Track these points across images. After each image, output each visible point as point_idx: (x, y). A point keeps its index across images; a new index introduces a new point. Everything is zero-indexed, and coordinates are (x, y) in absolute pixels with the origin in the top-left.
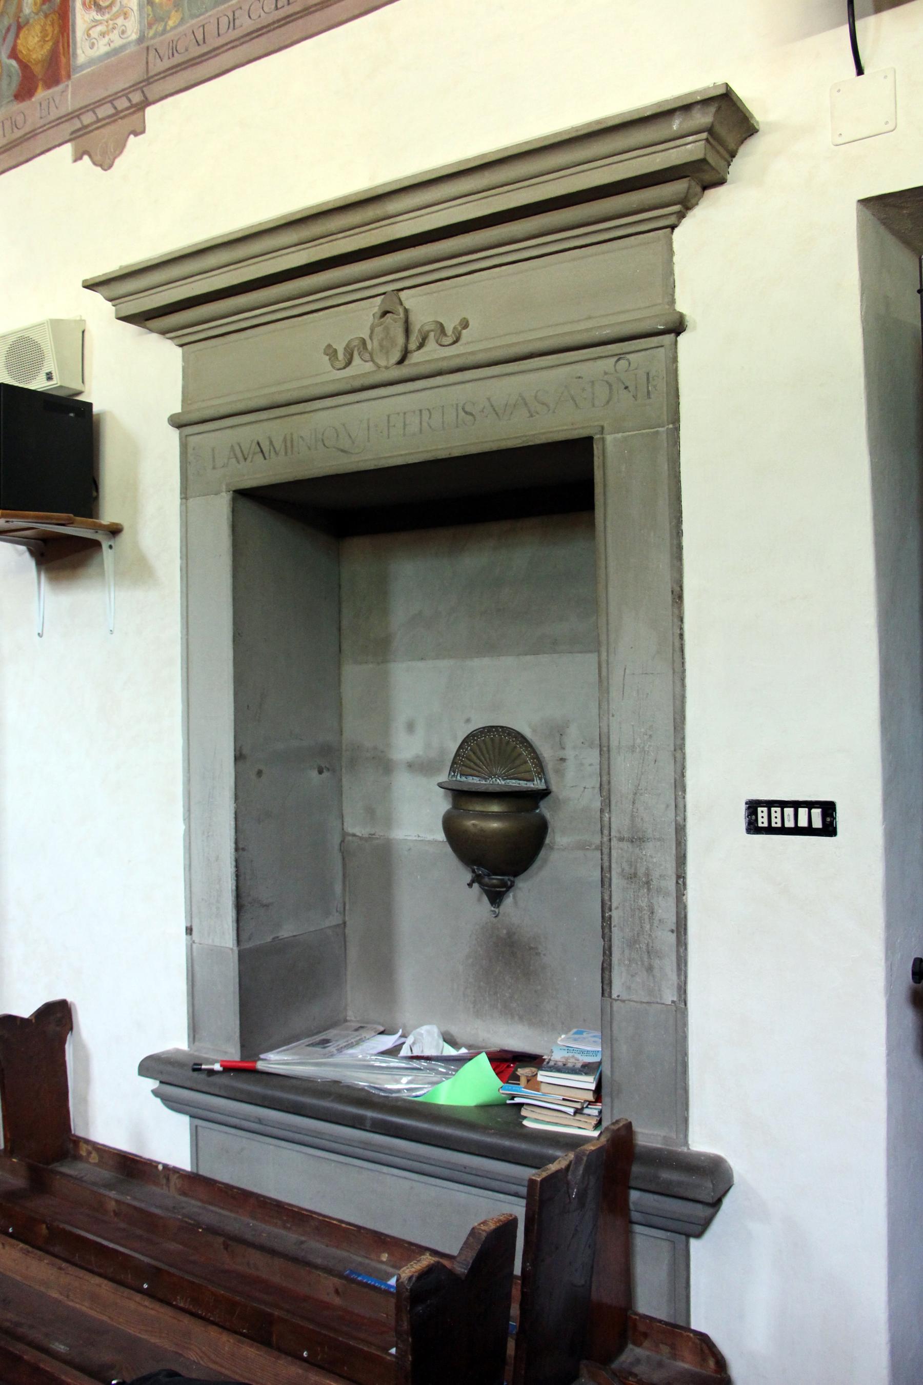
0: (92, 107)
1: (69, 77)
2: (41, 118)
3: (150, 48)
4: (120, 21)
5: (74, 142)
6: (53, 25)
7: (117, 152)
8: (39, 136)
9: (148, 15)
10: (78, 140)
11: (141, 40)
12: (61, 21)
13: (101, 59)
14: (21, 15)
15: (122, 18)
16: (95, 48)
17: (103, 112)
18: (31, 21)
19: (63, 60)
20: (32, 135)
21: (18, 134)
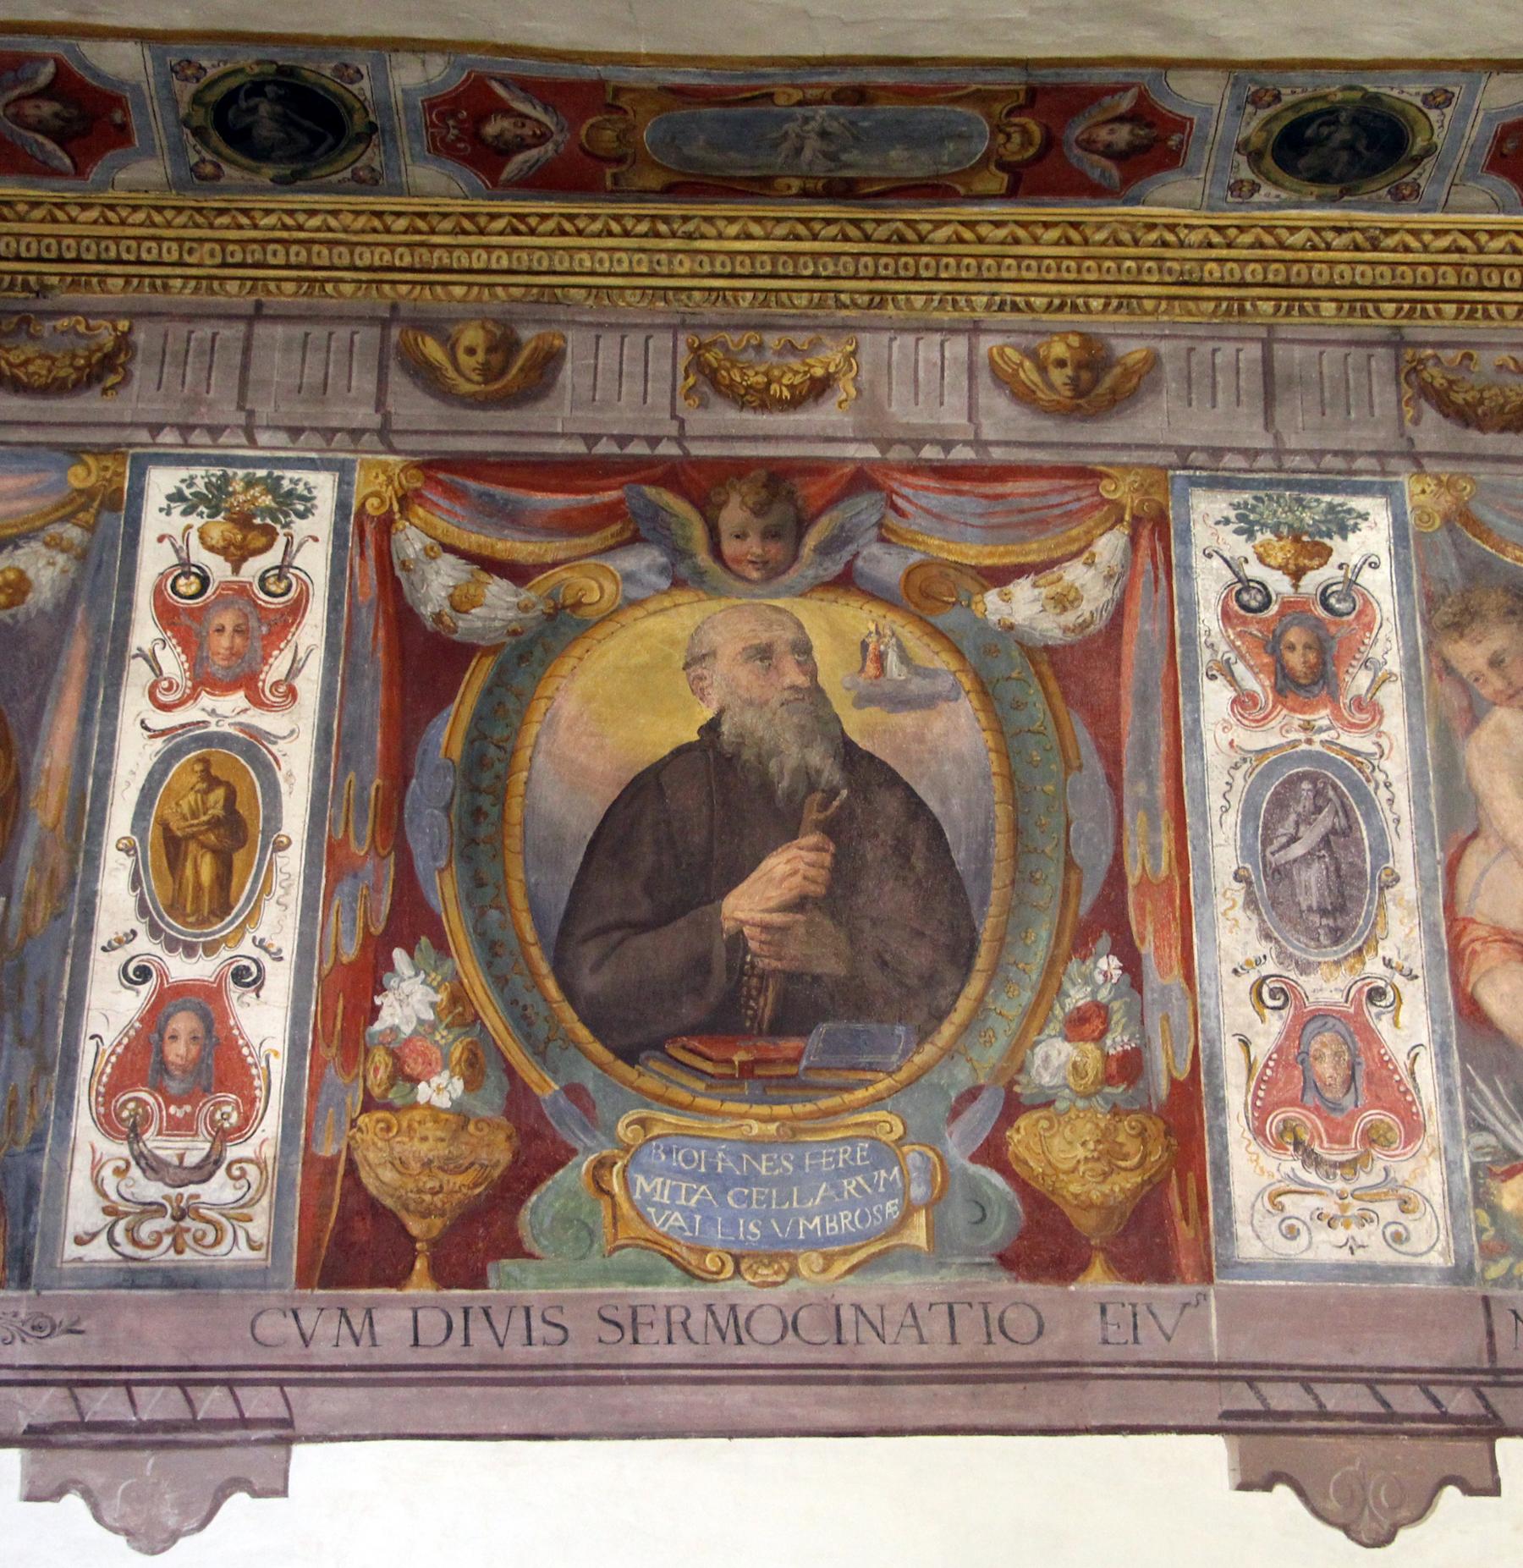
0: (1308, 1376)
1: (1208, 1278)
2: (1105, 1342)
3: (1494, 1307)
4: (1387, 1210)
5: (1235, 1439)
6: (1142, 1134)
7: (1404, 1513)
8: (1092, 1383)
9: (1480, 1231)
10: (1247, 1438)
11: (1461, 1273)
12: (1173, 1141)
13: (1318, 1271)
14: (1022, 1078)
15: (1395, 1205)
16: (1303, 1239)
17: (1335, 1398)
18: (1061, 1105)
19: (1185, 1232)
20: (1070, 1371)
21: (1001, 1351)
